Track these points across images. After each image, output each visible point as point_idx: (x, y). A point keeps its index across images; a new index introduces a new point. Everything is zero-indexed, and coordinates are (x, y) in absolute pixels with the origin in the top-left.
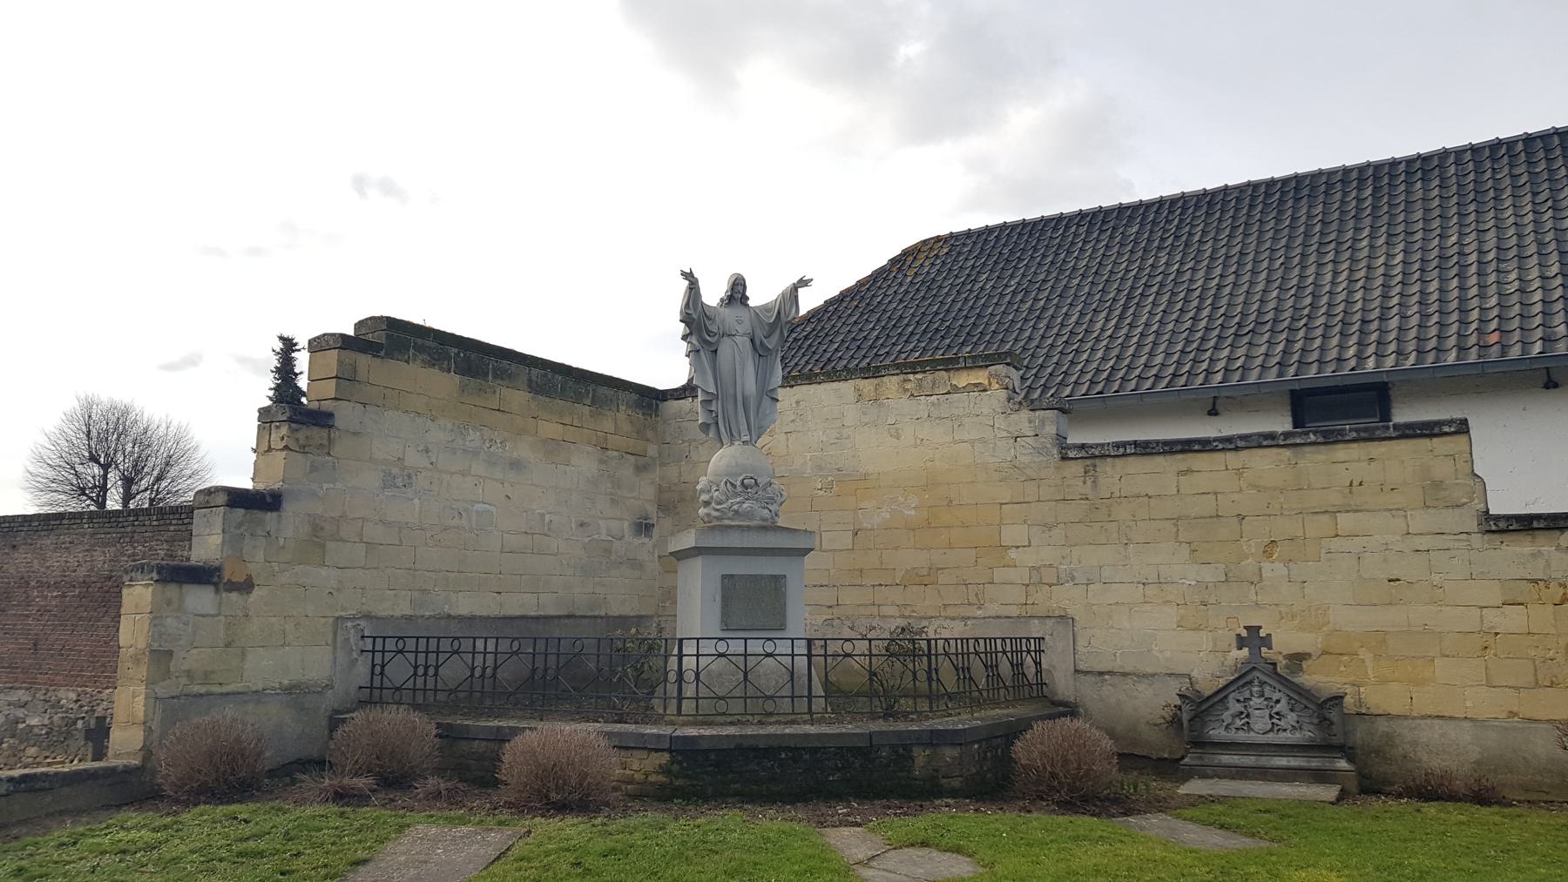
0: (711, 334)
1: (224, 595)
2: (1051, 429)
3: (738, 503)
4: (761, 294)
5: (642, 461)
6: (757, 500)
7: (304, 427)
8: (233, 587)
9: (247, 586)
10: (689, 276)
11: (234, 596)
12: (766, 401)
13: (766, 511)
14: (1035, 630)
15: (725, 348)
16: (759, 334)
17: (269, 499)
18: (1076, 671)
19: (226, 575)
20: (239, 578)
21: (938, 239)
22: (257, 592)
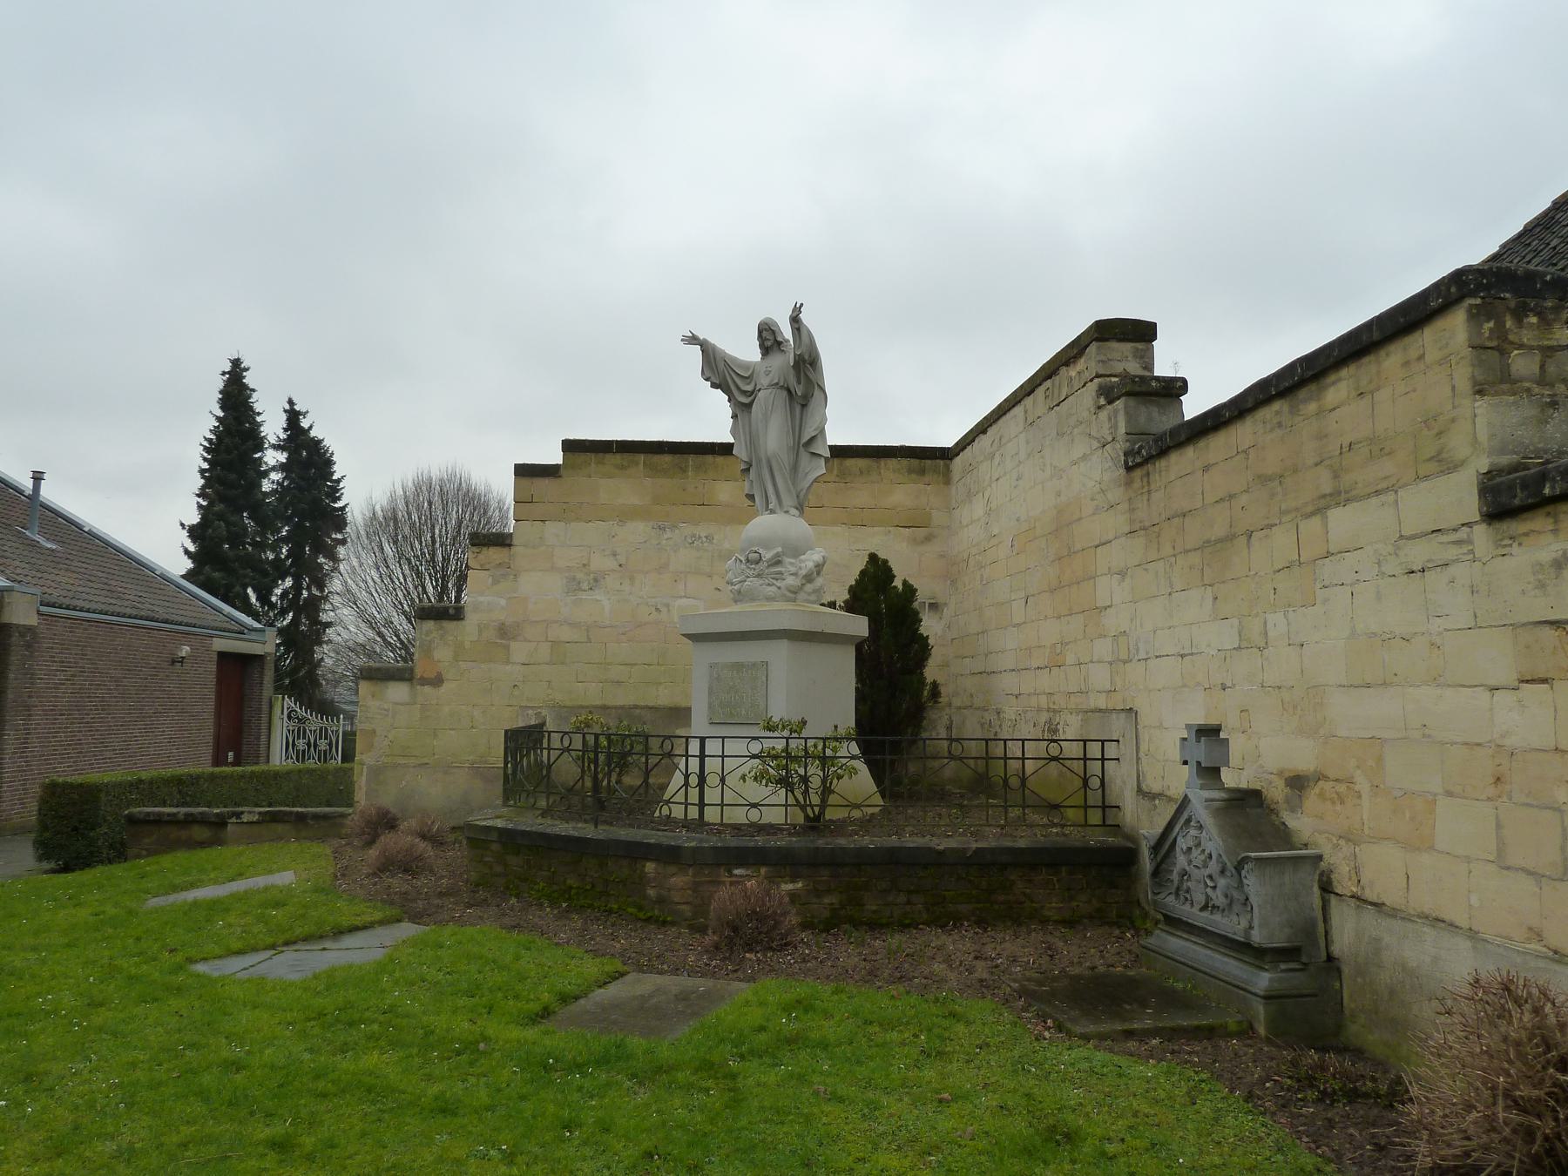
0: (748, 394)
1: (418, 687)
3: (740, 582)
5: (922, 532)
6: (758, 576)
7: (485, 549)
8: (424, 682)
9: (437, 681)
10: (693, 340)
11: (427, 689)
12: (804, 457)
13: (773, 589)
14: (1117, 726)
16: (792, 381)
17: (451, 611)
18: (1139, 790)
19: (418, 672)
20: (431, 675)
22: (446, 687)
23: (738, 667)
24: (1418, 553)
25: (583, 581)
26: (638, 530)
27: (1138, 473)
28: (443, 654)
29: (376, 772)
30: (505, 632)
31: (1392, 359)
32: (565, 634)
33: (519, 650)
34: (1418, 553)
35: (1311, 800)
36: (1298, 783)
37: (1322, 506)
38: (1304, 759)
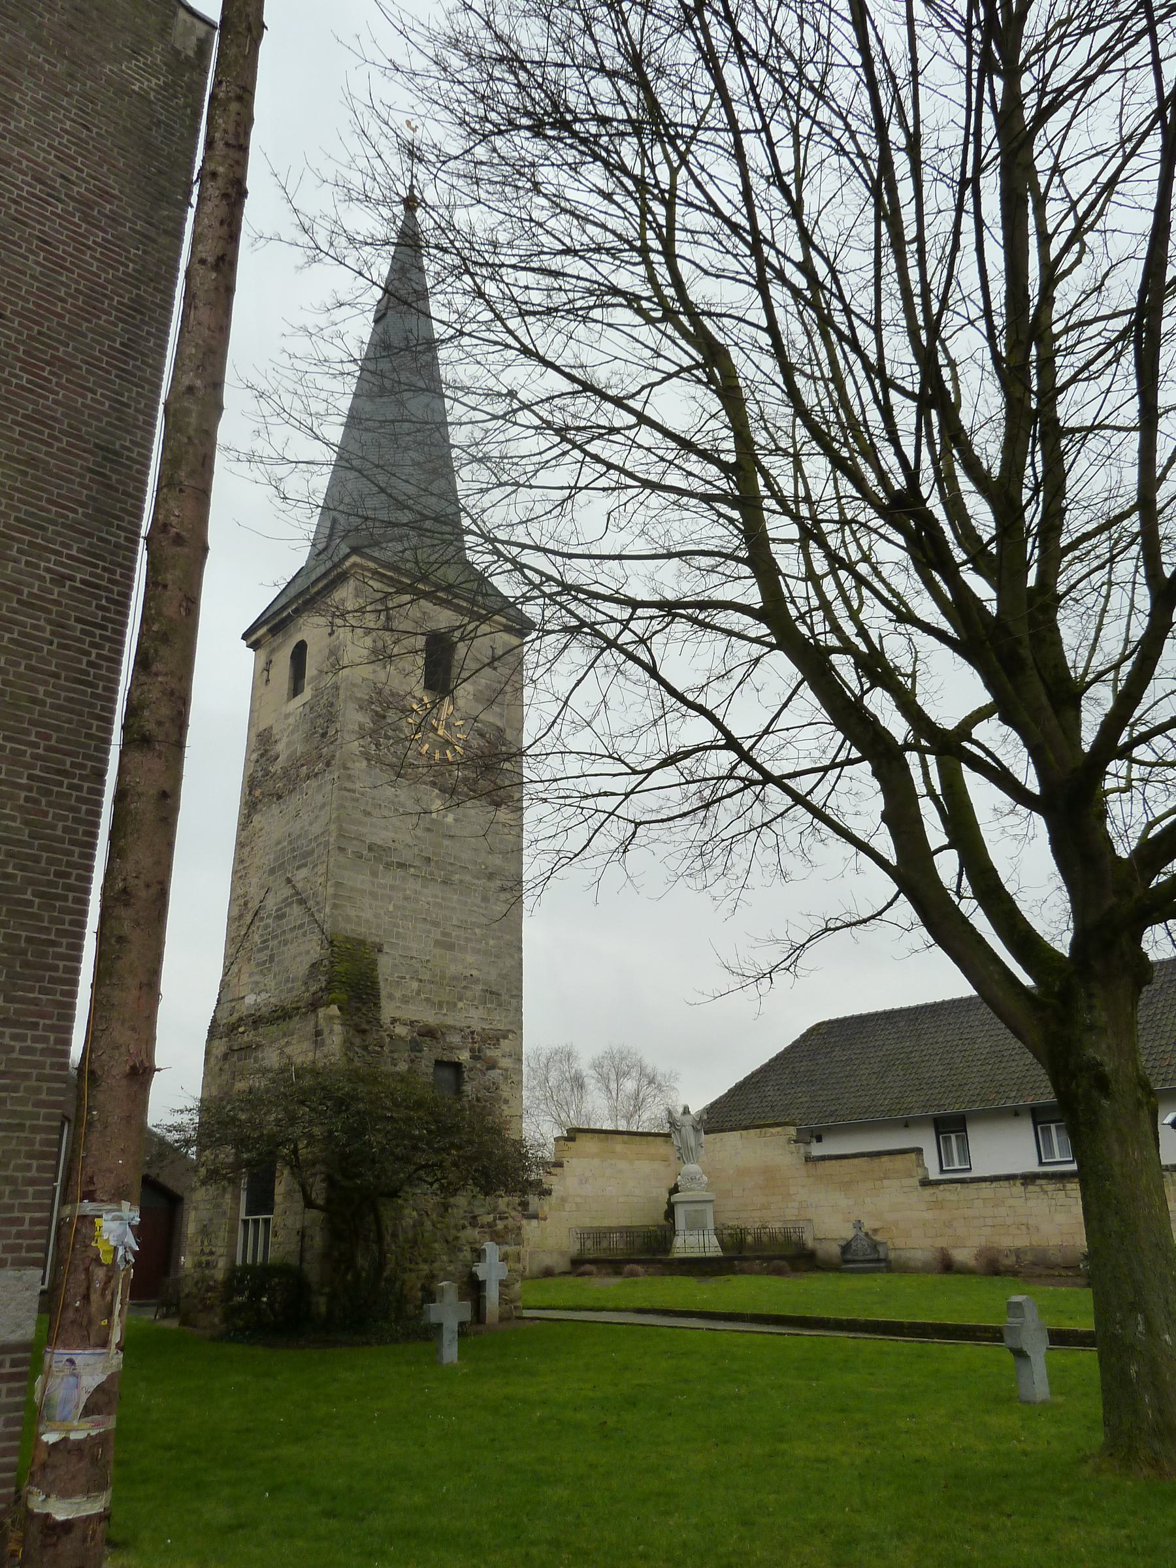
2: (802, 1151)
4: (695, 1109)
9: (545, 1219)
15: (683, 1130)
21: (823, 1023)
23: (696, 1211)
24: (906, 1189)
25: (583, 1181)
26: (596, 1162)
27: (810, 1164)
28: (546, 1208)
29: (531, 1254)
30: (563, 1200)
31: (899, 1157)
32: (578, 1200)
33: (567, 1206)
34: (906, 1189)
35: (880, 1233)
36: (875, 1231)
37: (881, 1179)
38: (877, 1225)
